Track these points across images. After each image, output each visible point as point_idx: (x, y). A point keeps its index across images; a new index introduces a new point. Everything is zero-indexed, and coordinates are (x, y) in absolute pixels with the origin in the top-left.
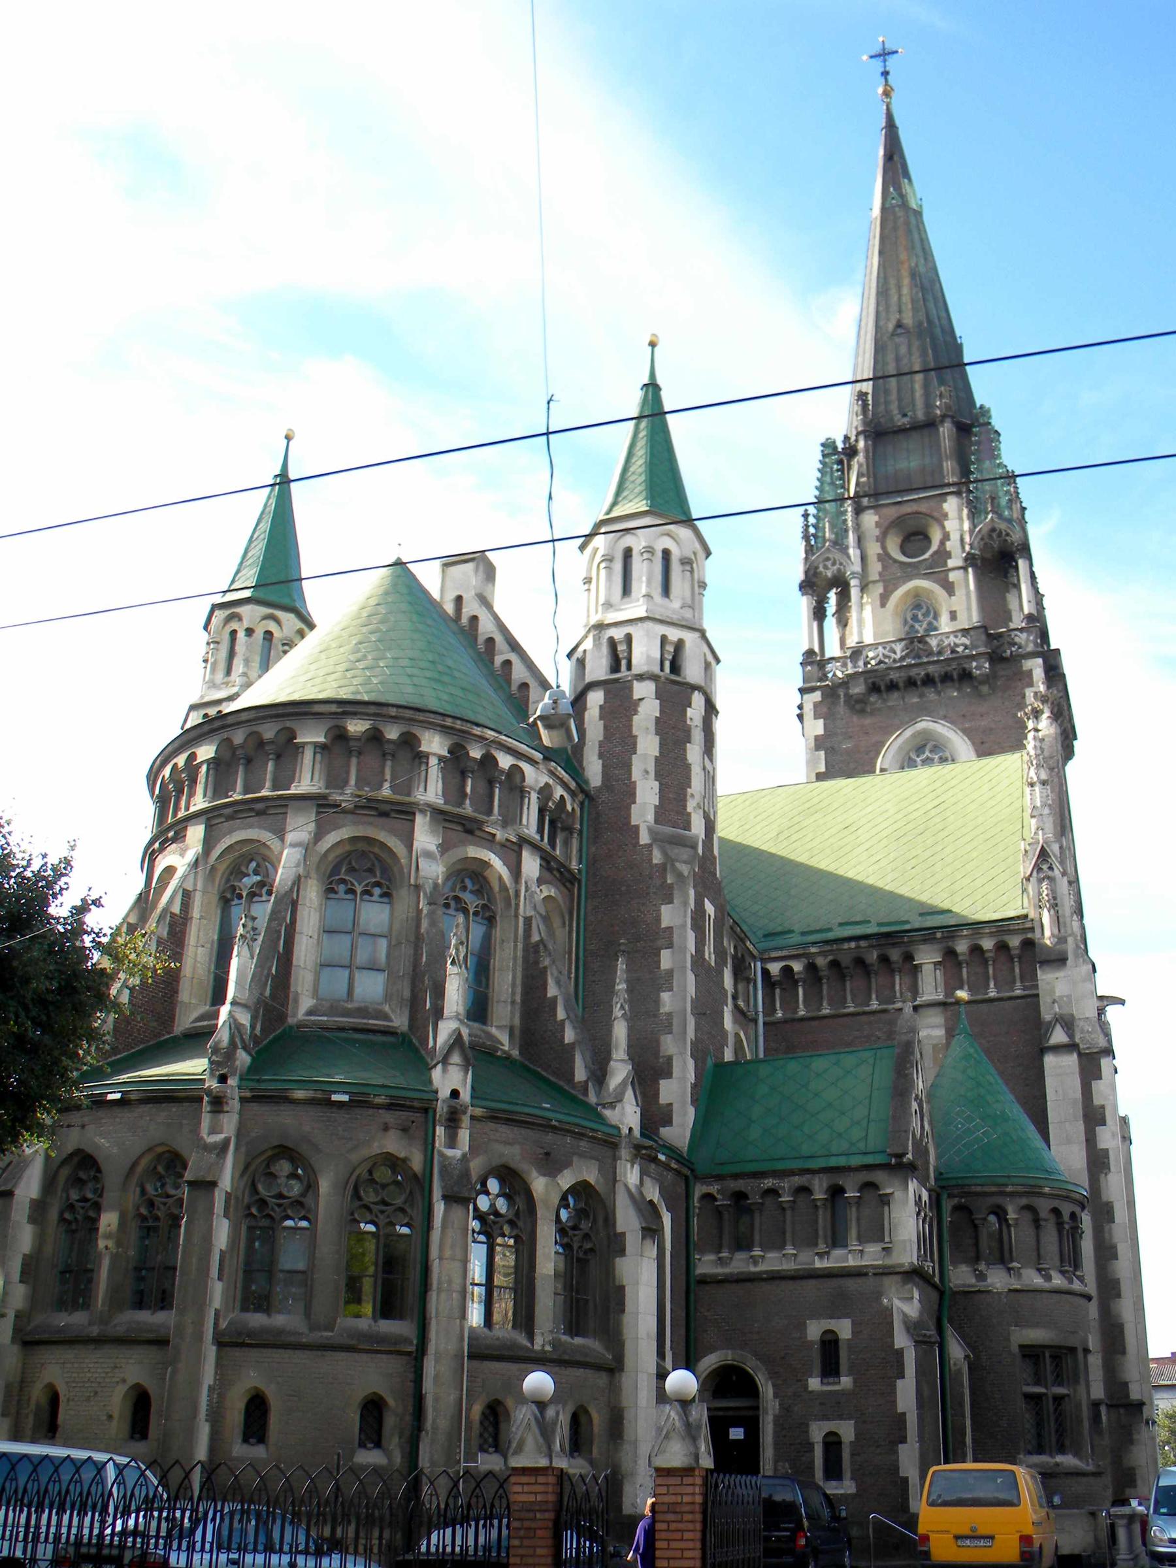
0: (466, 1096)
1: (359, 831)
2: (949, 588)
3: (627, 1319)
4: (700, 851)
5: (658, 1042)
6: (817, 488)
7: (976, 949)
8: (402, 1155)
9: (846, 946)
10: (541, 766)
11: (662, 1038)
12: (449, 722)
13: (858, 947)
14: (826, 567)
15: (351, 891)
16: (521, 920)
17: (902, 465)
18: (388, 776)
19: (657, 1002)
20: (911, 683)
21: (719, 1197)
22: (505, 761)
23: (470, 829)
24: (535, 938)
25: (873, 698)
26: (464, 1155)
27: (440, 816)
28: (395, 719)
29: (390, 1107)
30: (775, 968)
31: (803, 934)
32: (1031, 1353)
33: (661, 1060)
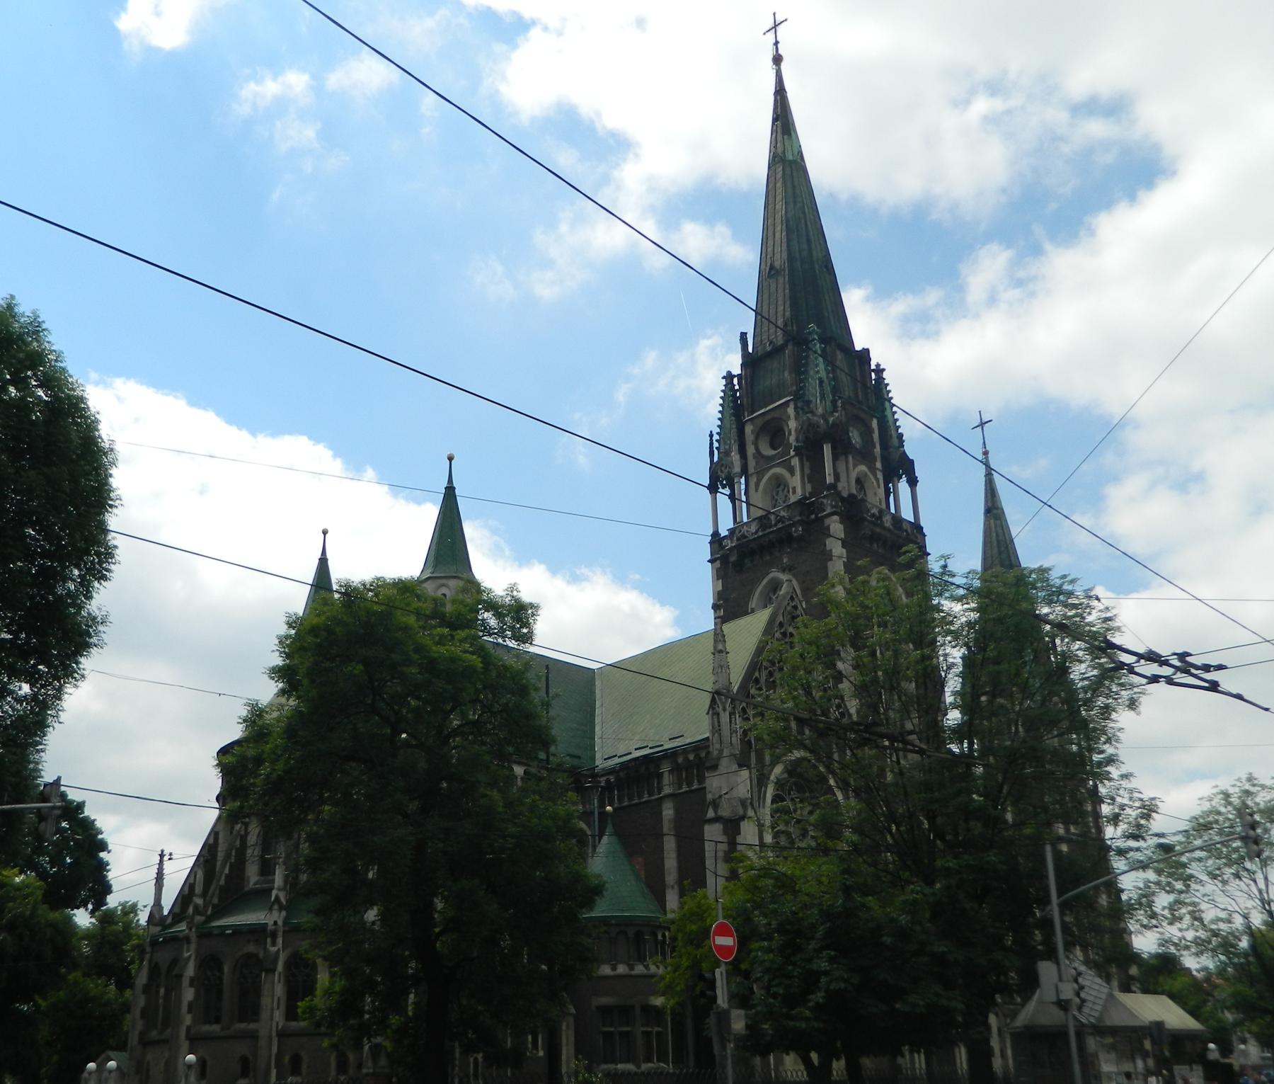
0: (280, 923)
2: (791, 471)
6: (720, 412)
14: (722, 471)
17: (768, 383)
26: (279, 950)
31: (620, 757)
32: (605, 1010)
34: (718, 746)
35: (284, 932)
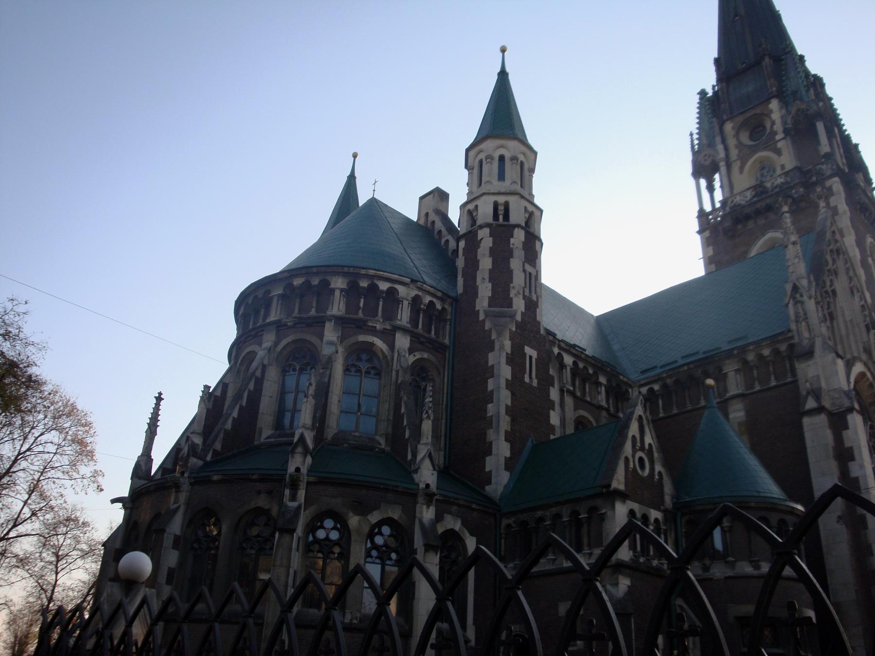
0: (304, 470)
1: (299, 336)
2: (778, 152)
3: (415, 601)
4: (519, 318)
5: (485, 434)
7: (761, 357)
8: (267, 507)
9: (681, 370)
10: (411, 286)
11: (488, 432)
12: (346, 269)
13: (689, 369)
15: (294, 370)
16: (394, 373)
18: (314, 305)
19: (485, 411)
20: (758, 213)
21: (514, 525)
22: (384, 286)
23: (361, 326)
24: (399, 381)
25: (739, 227)
26: (299, 507)
27: (340, 321)
28: (317, 274)
29: (261, 480)
30: (644, 390)
31: (661, 367)
33: (487, 445)
34: (806, 334)
35: (308, 483)
